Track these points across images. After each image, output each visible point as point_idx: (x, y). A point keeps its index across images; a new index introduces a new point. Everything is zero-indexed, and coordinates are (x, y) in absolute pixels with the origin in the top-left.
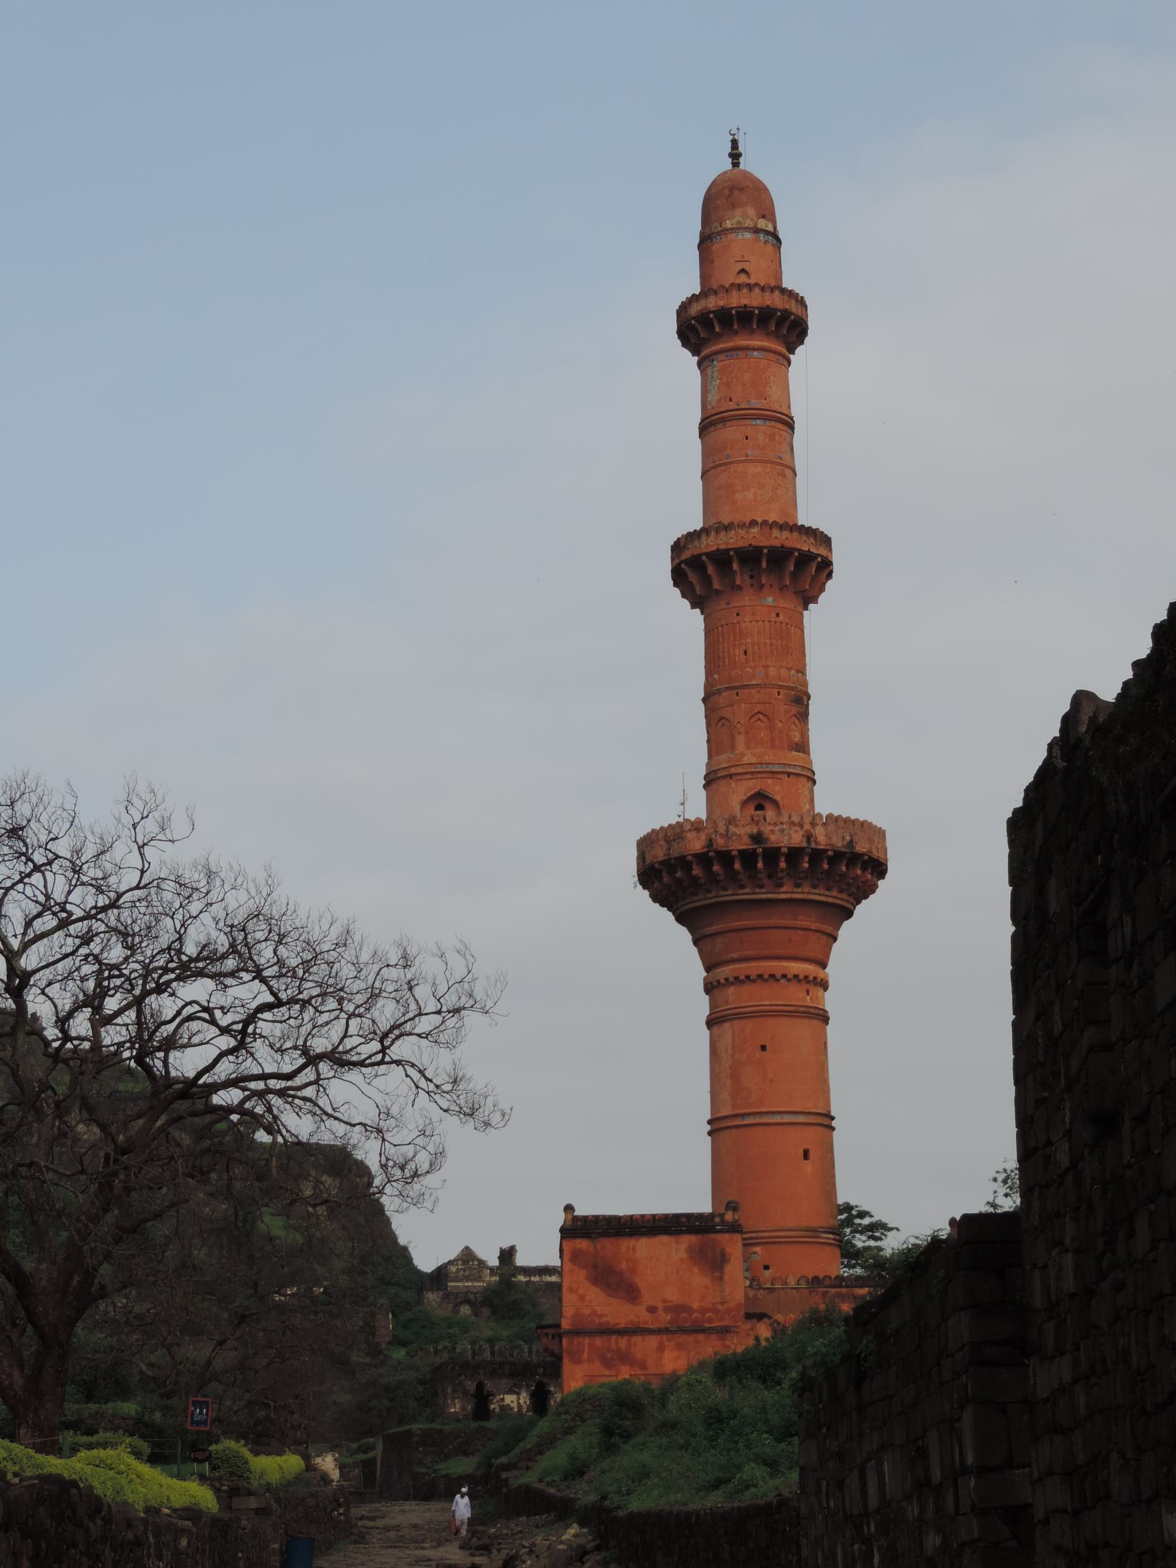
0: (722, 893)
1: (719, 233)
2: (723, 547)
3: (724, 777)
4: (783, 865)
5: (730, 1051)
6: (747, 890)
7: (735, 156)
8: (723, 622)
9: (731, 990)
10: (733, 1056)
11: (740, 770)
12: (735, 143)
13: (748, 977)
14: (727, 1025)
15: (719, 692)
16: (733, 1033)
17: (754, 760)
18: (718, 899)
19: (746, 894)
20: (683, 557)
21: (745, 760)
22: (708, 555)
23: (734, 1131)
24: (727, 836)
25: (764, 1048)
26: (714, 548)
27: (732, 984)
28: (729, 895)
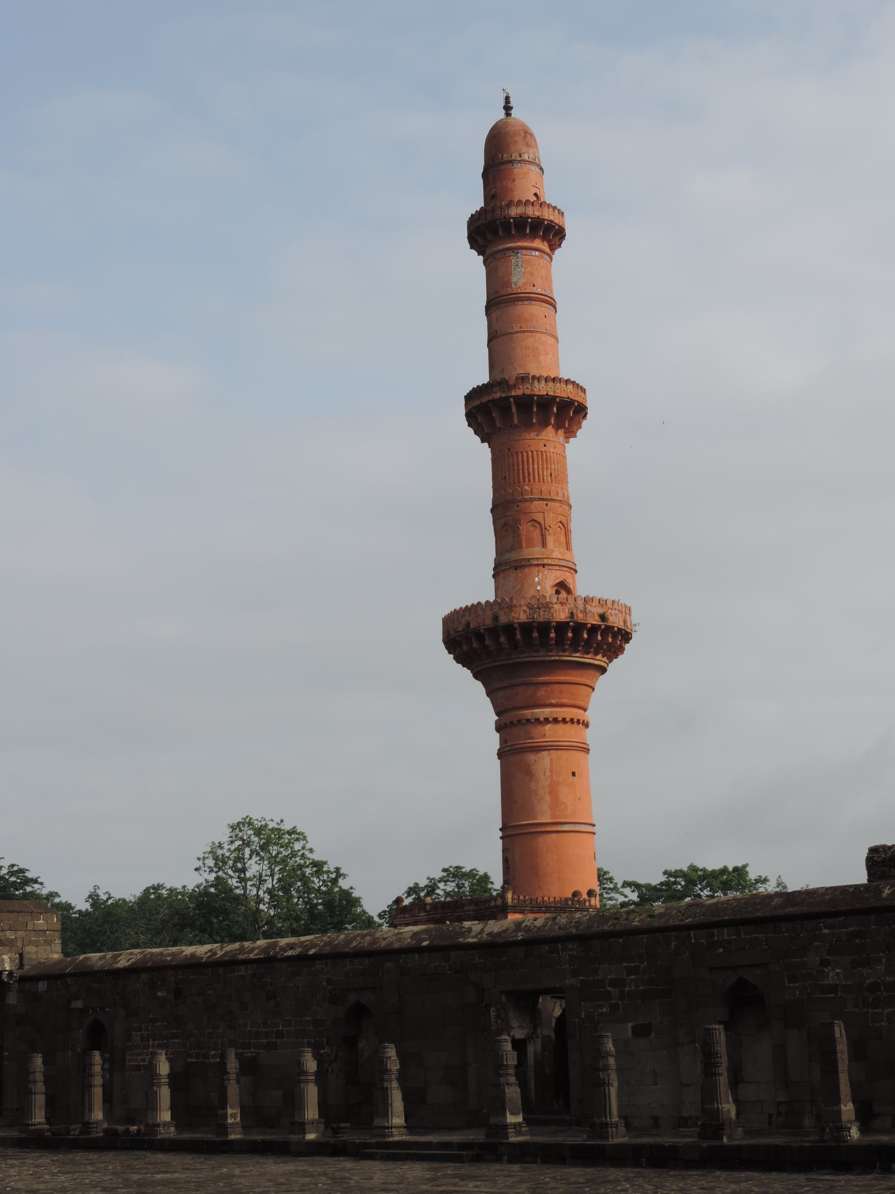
2: (552, 394)
3: (537, 565)
5: (548, 773)
7: (508, 108)
8: (533, 449)
9: (548, 727)
10: (551, 777)
11: (550, 562)
12: (507, 99)
14: (545, 753)
16: (551, 760)
17: (559, 556)
19: (577, 657)
20: (513, 393)
21: (554, 555)
23: (554, 835)
24: (584, 612)
25: (574, 774)
26: (545, 393)
27: (550, 722)
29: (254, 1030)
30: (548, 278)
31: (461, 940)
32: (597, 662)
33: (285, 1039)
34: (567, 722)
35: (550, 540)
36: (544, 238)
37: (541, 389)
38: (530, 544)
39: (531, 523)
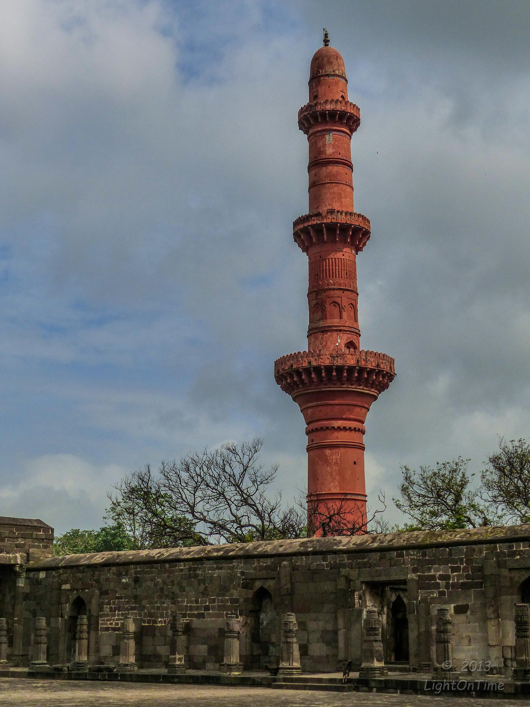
0: (350, 386)
1: (333, 75)
2: (349, 222)
3: (336, 330)
4: (345, 374)
6: (361, 387)
7: (326, 42)
11: (344, 328)
12: (326, 35)
13: (350, 428)
15: (334, 289)
17: (350, 325)
18: (347, 389)
20: (325, 221)
21: (347, 324)
22: (342, 224)
24: (366, 360)
25: (355, 463)
28: (352, 388)
29: (189, 605)
30: (348, 150)
31: (335, 547)
32: (372, 393)
33: (211, 611)
34: (352, 430)
35: (345, 315)
36: (347, 125)
37: (342, 219)
38: (332, 317)
39: (333, 304)
